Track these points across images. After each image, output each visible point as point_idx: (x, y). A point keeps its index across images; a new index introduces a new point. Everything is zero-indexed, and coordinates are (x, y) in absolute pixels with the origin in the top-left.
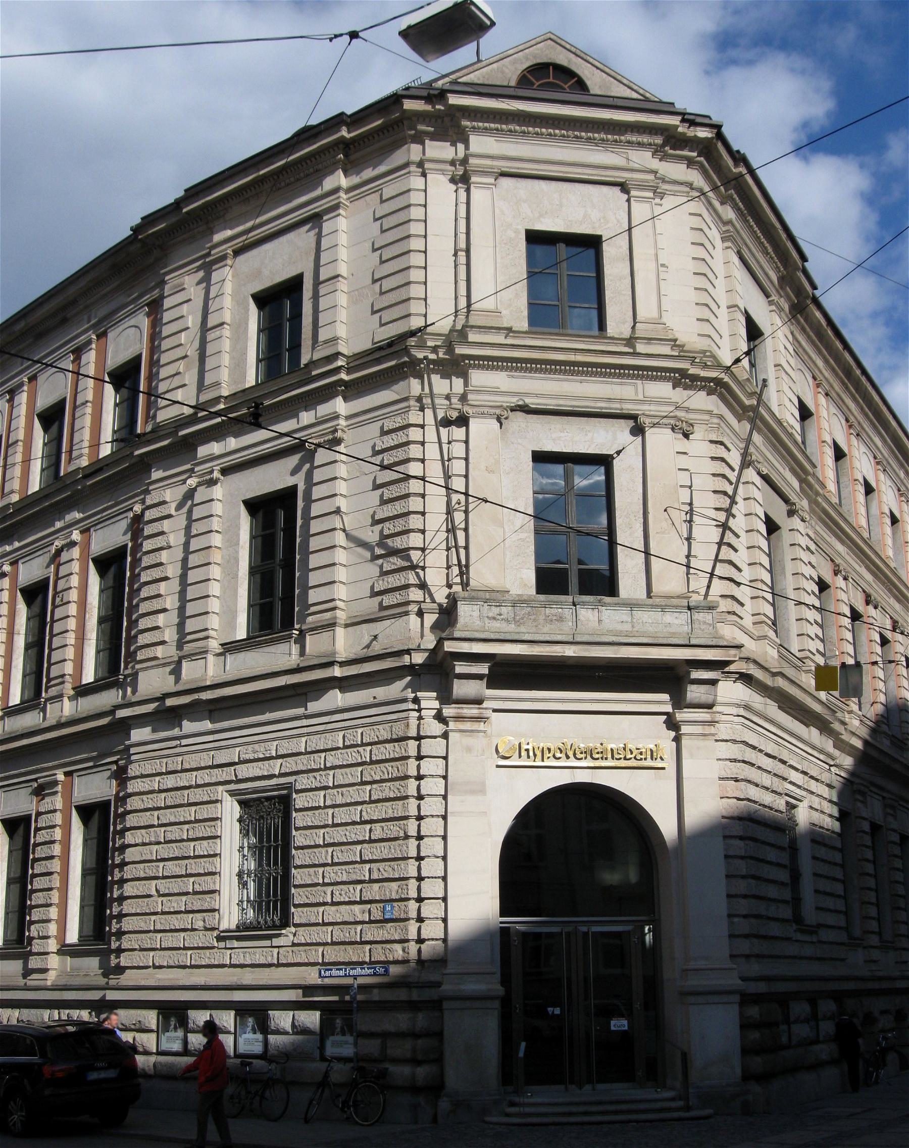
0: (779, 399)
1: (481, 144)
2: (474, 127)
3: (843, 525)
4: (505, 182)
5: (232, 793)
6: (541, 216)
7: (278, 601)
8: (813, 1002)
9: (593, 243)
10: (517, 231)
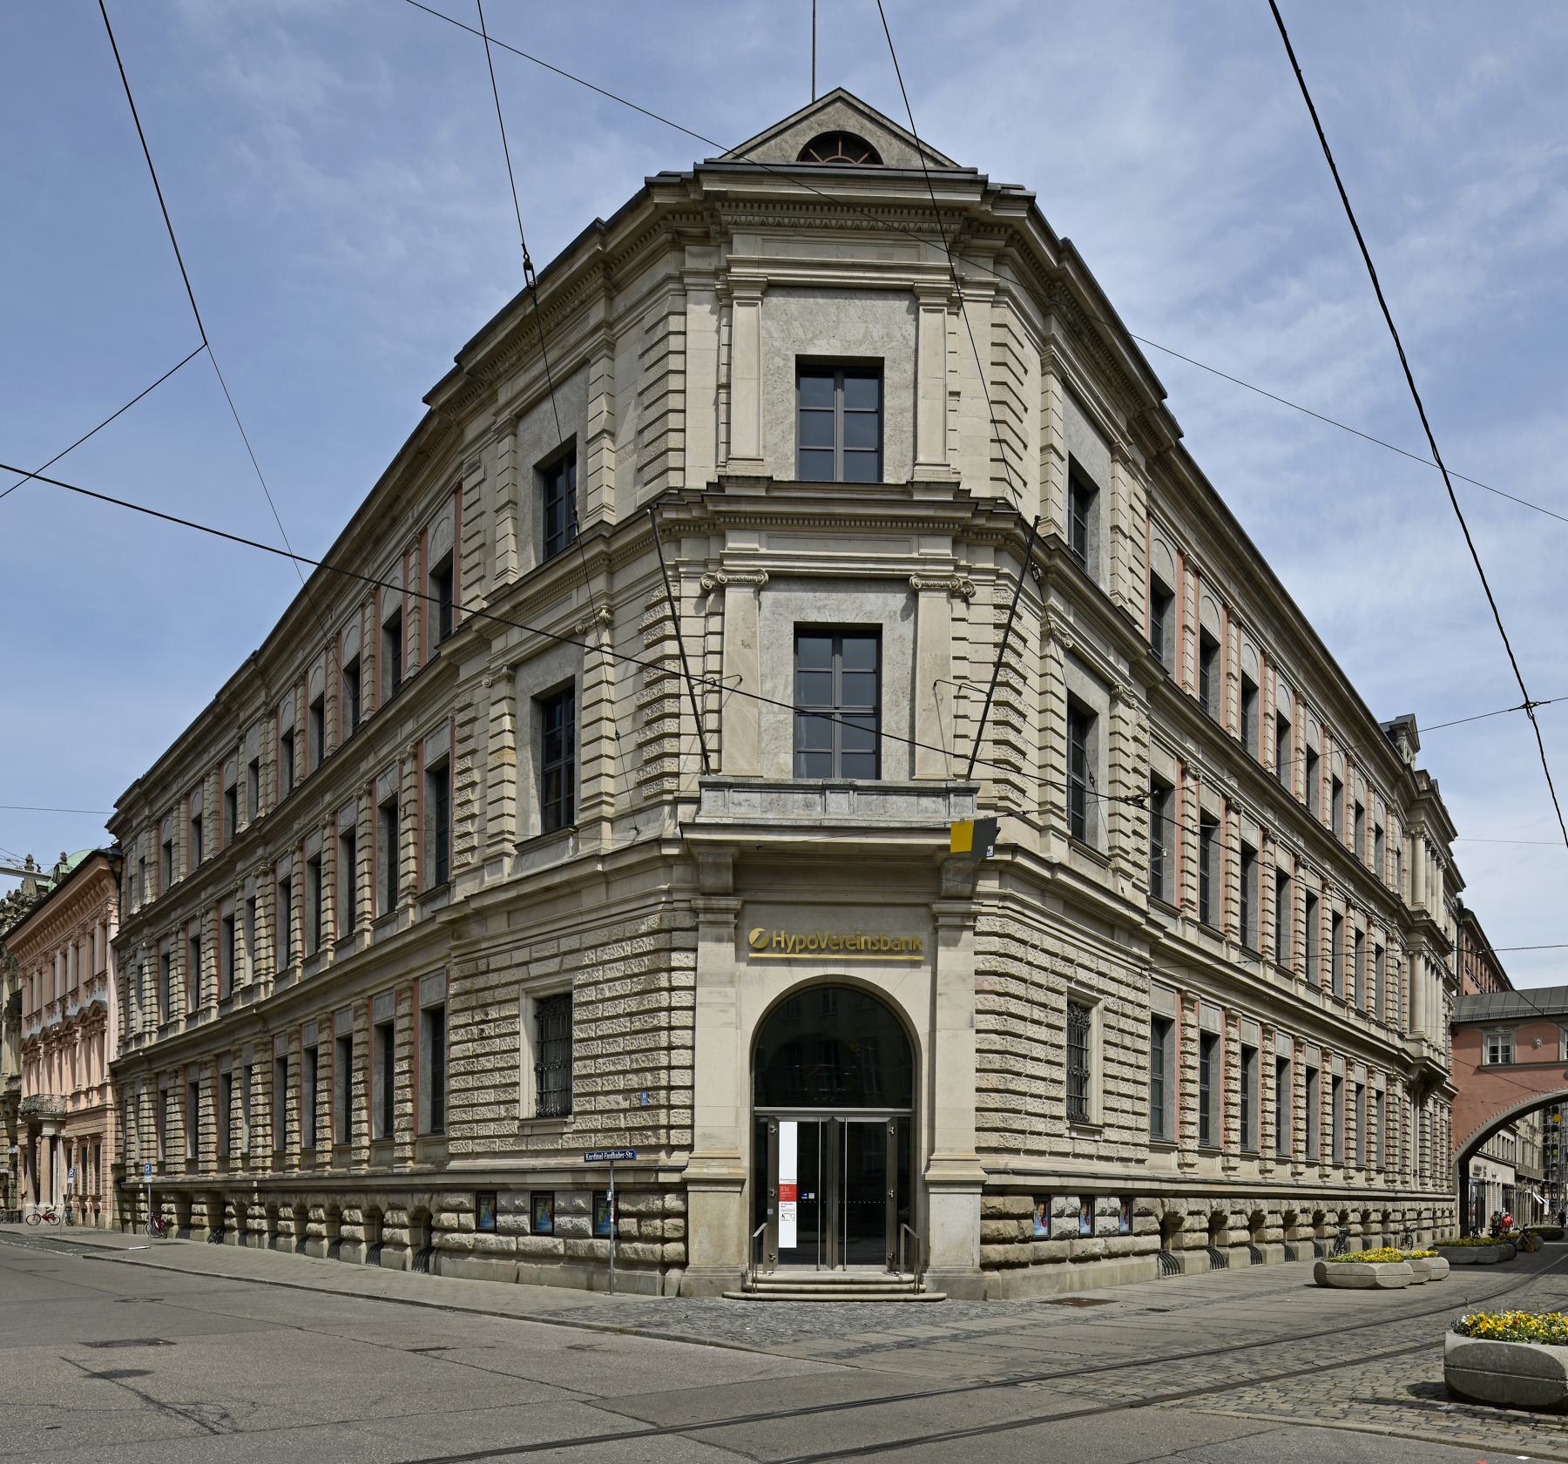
0: (1112, 568)
1: (744, 247)
2: (735, 223)
3: (1198, 721)
4: (776, 301)
5: (528, 992)
6: (815, 336)
7: (1494, 1059)
8: (1088, 1198)
9: (871, 369)
10: (786, 359)
